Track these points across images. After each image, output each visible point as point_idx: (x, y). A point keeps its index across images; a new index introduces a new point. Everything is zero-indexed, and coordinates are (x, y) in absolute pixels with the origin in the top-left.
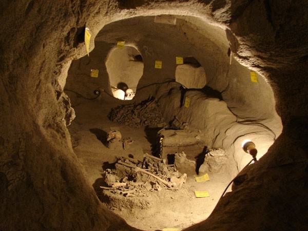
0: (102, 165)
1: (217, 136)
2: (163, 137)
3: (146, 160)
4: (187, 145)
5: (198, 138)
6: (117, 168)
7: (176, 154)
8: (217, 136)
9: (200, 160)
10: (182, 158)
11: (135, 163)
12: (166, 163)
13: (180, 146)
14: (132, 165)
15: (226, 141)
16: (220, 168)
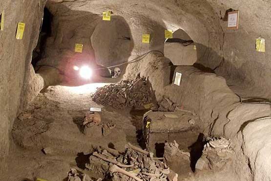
0: (75, 158)
1: (216, 120)
2: (150, 120)
3: (128, 152)
4: (179, 132)
5: (192, 122)
6: (91, 162)
7: (166, 144)
8: (216, 120)
9: (197, 150)
10: (173, 148)
11: (114, 156)
12: (154, 156)
13: (171, 132)
14: (111, 159)
15: (228, 127)
16: (225, 165)
